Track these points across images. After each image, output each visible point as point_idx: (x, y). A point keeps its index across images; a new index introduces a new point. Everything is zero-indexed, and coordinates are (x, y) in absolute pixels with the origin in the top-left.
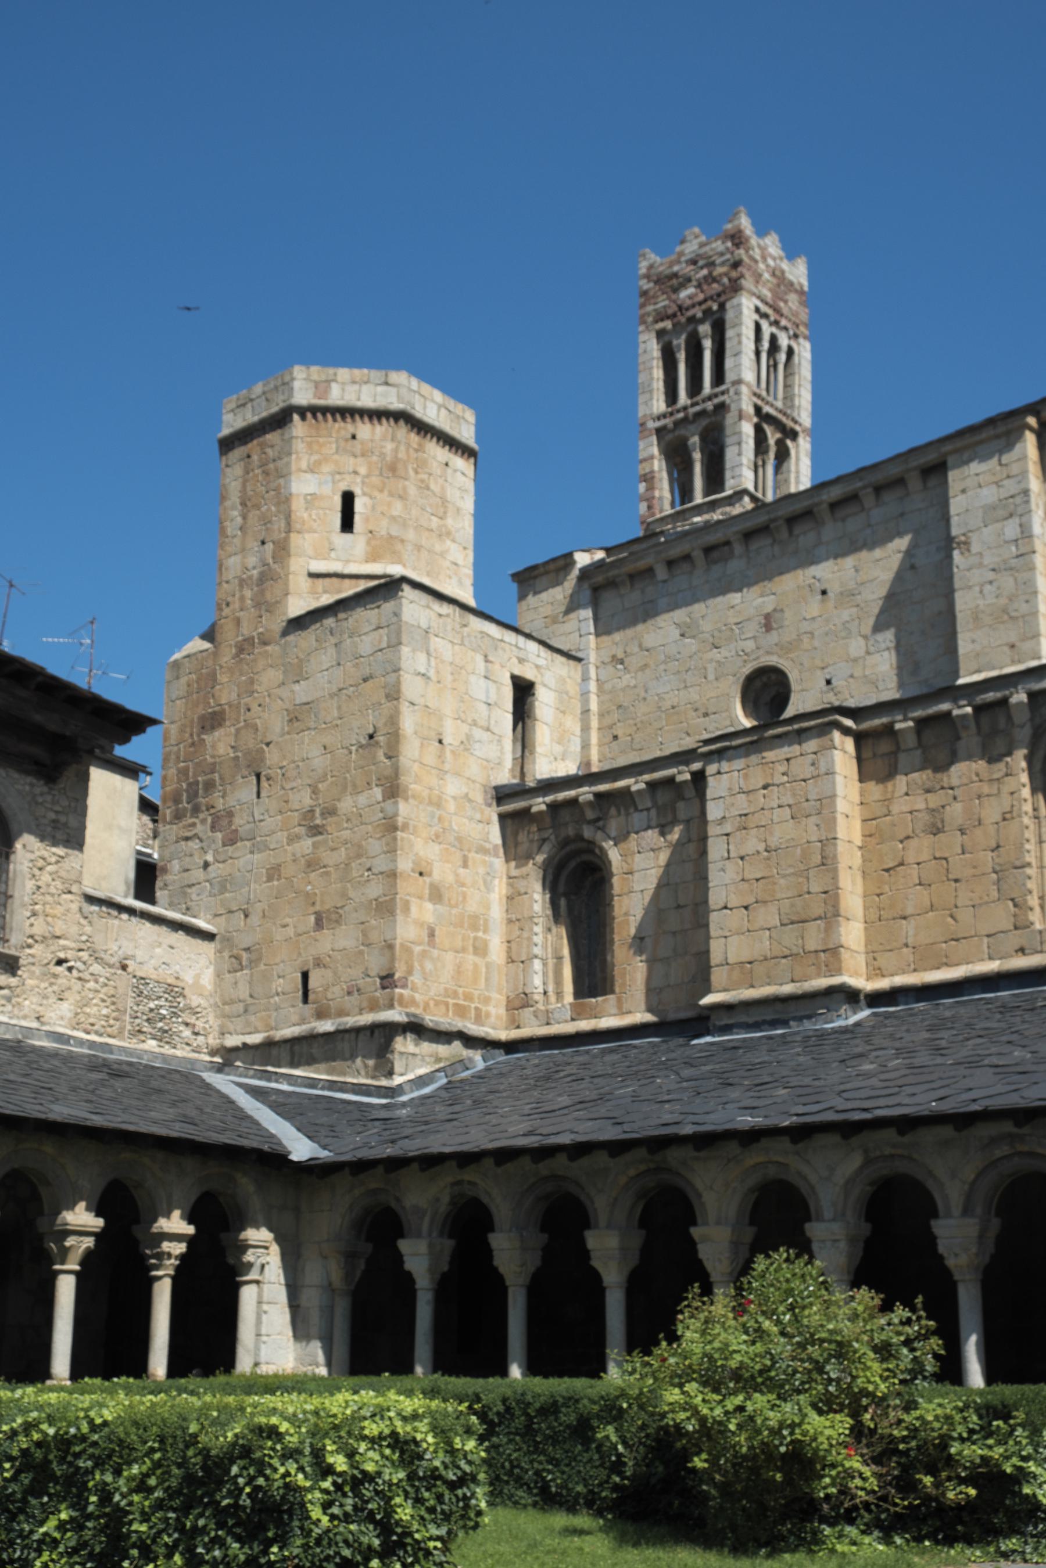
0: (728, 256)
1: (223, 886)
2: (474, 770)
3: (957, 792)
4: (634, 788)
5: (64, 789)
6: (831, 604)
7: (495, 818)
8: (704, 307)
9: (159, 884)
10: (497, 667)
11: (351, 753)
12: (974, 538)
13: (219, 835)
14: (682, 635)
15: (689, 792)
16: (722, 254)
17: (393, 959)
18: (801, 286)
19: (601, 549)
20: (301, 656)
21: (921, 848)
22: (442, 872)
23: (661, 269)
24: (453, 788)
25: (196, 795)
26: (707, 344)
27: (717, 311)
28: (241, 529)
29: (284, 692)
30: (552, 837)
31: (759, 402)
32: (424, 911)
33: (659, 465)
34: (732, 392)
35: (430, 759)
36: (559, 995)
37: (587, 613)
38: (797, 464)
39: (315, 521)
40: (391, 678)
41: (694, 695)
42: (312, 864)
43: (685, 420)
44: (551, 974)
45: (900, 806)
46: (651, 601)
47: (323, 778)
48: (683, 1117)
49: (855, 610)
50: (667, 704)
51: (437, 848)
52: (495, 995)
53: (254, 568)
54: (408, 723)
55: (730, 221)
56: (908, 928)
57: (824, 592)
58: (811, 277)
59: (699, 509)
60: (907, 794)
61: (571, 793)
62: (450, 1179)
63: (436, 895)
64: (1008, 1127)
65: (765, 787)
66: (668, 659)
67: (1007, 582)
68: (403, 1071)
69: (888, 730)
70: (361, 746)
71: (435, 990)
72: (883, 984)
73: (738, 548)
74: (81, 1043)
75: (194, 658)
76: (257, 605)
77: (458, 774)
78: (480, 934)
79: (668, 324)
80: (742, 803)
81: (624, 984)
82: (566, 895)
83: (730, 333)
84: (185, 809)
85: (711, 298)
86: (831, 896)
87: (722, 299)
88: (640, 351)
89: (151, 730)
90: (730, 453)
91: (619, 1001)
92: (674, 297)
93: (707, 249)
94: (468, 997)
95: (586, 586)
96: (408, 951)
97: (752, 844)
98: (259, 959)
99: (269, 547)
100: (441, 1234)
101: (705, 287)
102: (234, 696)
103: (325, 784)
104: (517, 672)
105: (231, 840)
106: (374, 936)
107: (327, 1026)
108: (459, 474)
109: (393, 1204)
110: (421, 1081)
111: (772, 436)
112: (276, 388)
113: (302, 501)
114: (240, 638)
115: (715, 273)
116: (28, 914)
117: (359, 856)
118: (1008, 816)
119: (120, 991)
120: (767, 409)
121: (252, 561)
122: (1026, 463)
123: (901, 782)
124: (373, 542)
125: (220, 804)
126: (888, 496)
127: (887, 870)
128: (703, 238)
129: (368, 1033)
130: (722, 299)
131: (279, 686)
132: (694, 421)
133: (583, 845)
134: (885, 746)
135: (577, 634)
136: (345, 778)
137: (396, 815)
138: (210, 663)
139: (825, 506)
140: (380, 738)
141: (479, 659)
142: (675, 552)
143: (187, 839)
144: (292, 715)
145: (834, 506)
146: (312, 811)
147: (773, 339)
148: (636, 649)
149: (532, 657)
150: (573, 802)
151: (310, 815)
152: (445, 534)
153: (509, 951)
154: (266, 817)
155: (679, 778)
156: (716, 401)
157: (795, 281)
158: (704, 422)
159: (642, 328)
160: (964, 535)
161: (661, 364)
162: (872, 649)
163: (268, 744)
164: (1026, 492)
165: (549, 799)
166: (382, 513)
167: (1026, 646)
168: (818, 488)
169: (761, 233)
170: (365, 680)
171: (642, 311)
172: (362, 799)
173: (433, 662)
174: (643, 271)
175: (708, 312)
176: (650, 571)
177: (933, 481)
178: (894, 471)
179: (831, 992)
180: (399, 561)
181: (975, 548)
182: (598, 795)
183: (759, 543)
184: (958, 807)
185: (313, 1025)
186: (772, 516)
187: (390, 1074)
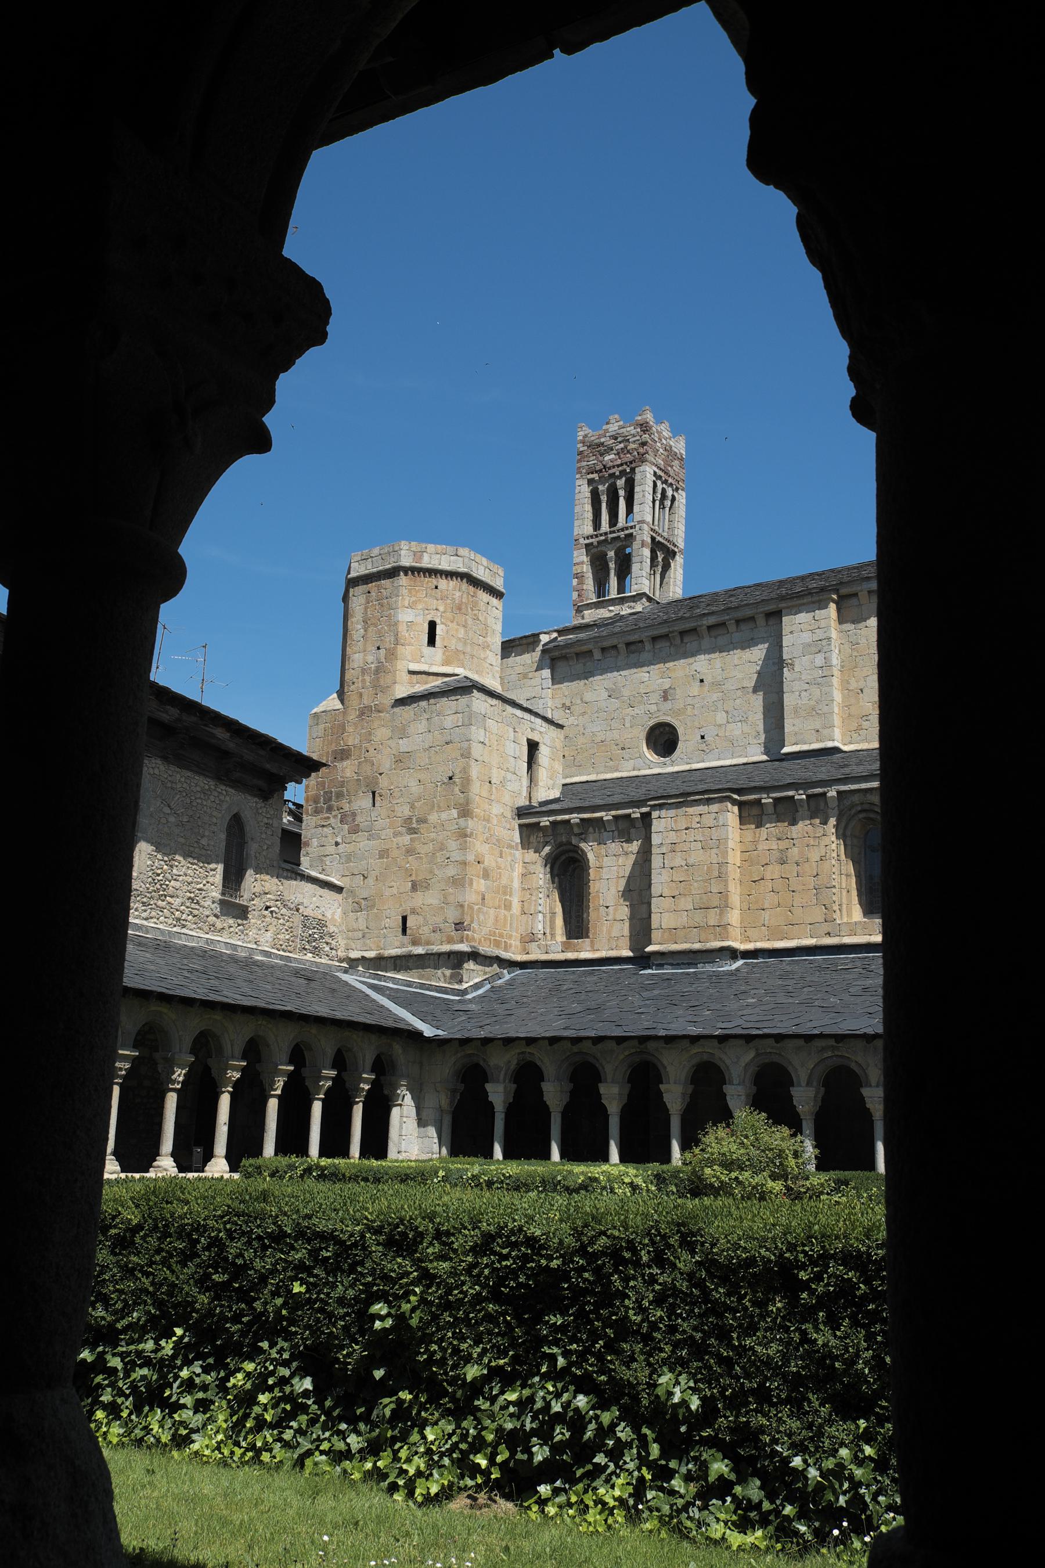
0: (638, 438)
1: (349, 858)
2: (507, 798)
3: (795, 842)
4: (605, 819)
6: (706, 689)
7: (517, 827)
9: (303, 852)
10: (520, 734)
12: (797, 662)
13: (346, 826)
15: (639, 824)
16: (634, 436)
17: (463, 914)
18: (681, 454)
19: (555, 631)
21: (774, 871)
22: (489, 861)
23: (592, 438)
24: (496, 810)
25: (330, 799)
26: (622, 493)
30: (552, 841)
31: (654, 535)
32: (480, 885)
33: (587, 569)
34: (637, 527)
35: (485, 794)
36: (553, 935)
37: (546, 673)
38: (675, 573)
40: (465, 745)
41: (615, 734)
42: (410, 851)
43: (606, 540)
44: (548, 923)
45: (763, 846)
48: (656, 1024)
50: (598, 739)
51: (487, 846)
52: (514, 934)
54: (474, 771)
56: (766, 916)
57: (702, 681)
58: (687, 448)
59: (613, 602)
60: (767, 839)
61: (567, 817)
62: (518, 1051)
63: (486, 875)
64: (832, 1042)
65: (686, 829)
67: (816, 692)
68: (467, 980)
69: (758, 802)
71: (485, 931)
72: (750, 946)
73: (648, 646)
74: (277, 956)
76: (375, 687)
77: (498, 802)
78: (508, 897)
79: (595, 476)
80: (672, 837)
81: (595, 933)
82: (557, 876)
83: (637, 489)
85: (626, 463)
86: (724, 895)
87: (633, 465)
88: (577, 491)
89: (323, 770)
90: (635, 568)
91: (592, 942)
92: (601, 458)
93: (623, 430)
94: (501, 935)
95: (547, 657)
96: (471, 908)
97: (678, 861)
98: (373, 906)
99: (382, 651)
100: (510, 1081)
101: (622, 456)
102: (357, 741)
105: (355, 830)
106: (451, 899)
107: (420, 950)
109: (481, 1063)
110: (477, 986)
112: (389, 553)
115: (629, 448)
116: (253, 880)
117: (441, 849)
118: (823, 858)
119: (295, 924)
120: (658, 538)
121: (370, 658)
122: (830, 621)
123: (763, 832)
125: (346, 807)
126: (744, 627)
127: (754, 882)
128: (621, 423)
129: (446, 957)
130: (633, 465)
132: (610, 543)
133: (572, 848)
134: (755, 811)
135: (540, 687)
137: (467, 827)
138: (341, 718)
139: (705, 627)
141: (511, 730)
142: (606, 644)
143: (323, 826)
145: (710, 628)
146: (410, 819)
147: (664, 491)
148: (579, 702)
150: (568, 821)
151: (409, 821)
152: (486, 647)
153: (523, 907)
154: (379, 818)
155: (633, 816)
156: (627, 532)
159: (578, 476)
162: (730, 720)
163: (381, 774)
164: (829, 639)
165: (551, 819)
167: (825, 732)
168: (690, 602)
169: (659, 422)
171: (579, 465)
172: (444, 816)
174: (581, 438)
175: (623, 473)
176: (590, 652)
178: (748, 612)
179: (722, 949)
181: (797, 669)
182: (582, 820)
183: (662, 644)
184: (795, 850)
185: (410, 948)
187: (461, 981)
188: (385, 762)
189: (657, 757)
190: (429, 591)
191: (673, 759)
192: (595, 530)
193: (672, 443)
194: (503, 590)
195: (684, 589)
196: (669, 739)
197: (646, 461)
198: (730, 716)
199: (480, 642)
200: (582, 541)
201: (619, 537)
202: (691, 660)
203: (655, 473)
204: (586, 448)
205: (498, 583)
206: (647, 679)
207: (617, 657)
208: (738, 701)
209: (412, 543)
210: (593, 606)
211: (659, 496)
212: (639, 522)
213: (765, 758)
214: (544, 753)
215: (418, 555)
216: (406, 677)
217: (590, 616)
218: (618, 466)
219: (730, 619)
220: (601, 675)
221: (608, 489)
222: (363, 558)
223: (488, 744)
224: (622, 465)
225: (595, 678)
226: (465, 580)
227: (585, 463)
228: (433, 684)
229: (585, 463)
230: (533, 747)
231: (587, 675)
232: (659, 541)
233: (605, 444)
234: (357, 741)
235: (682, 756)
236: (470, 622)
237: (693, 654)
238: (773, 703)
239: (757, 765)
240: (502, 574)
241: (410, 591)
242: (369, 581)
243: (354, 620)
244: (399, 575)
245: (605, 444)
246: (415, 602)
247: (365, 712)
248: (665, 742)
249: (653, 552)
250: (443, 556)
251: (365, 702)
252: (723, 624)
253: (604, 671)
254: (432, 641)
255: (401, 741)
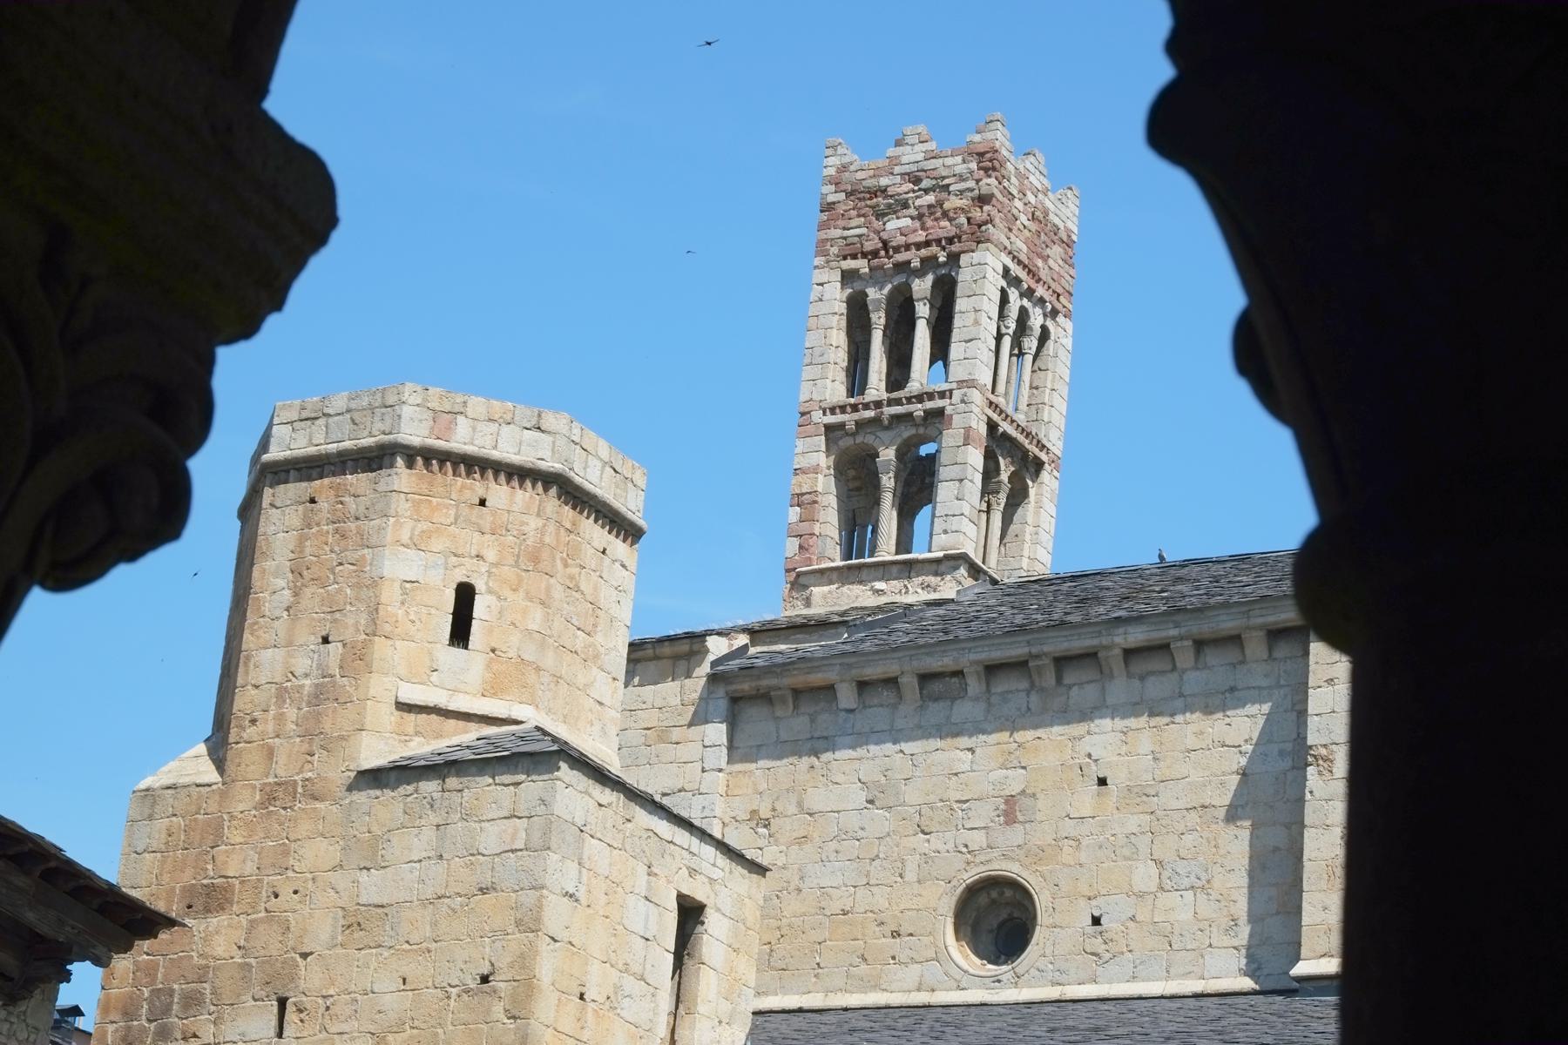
0: (971, 184)
5: (25, 1013)
8: (924, 252)
10: (662, 882)
11: (449, 998)
14: (871, 802)
16: (962, 179)
18: (1069, 232)
19: (745, 630)
20: (374, 829)
23: (860, 175)
25: (167, 1010)
26: (923, 310)
27: (944, 264)
28: (288, 609)
29: (340, 879)
31: (995, 417)
33: (825, 486)
34: (957, 395)
37: (717, 732)
38: (1037, 514)
39: (414, 622)
40: (529, 898)
41: (880, 899)
43: (876, 421)
46: (826, 738)
47: (398, 1028)
49: (1148, 817)
50: (836, 907)
53: (306, 675)
54: (547, 966)
55: (978, 132)
57: (1102, 782)
66: (843, 835)
70: (467, 991)
73: (974, 685)
75: (184, 792)
79: (861, 265)
83: (961, 304)
84: (143, 1030)
85: (938, 241)
87: (955, 248)
89: (164, 936)
90: (945, 492)
92: (877, 224)
95: (721, 691)
99: (335, 649)
101: (929, 223)
102: (250, 868)
103: (399, 1037)
104: (685, 891)
108: (617, 564)
111: (1006, 470)
113: (397, 585)
114: (271, 780)
115: (947, 206)
120: (1004, 426)
121: (302, 663)
124: (495, 667)
126: (1212, 657)
128: (932, 146)
130: (955, 248)
131: (334, 869)
132: (887, 428)
135: (698, 766)
136: (436, 1034)
138: (213, 807)
139: (1117, 651)
140: (497, 983)
142: (873, 672)
144: (352, 920)
145: (1129, 653)
147: (1023, 315)
148: (792, 809)
149: (705, 867)
152: (590, 658)
156: (929, 405)
157: (1061, 226)
158: (907, 432)
159: (819, 261)
160: (1325, 746)
161: (844, 323)
162: (1168, 884)
163: (305, 956)
166: (514, 624)
170: (483, 891)
171: (823, 235)
173: (585, 879)
174: (832, 171)
175: (929, 263)
176: (830, 689)
177: (1284, 649)
178: (1227, 623)
180: (533, 703)
186: (1034, 650)
188: (321, 929)
189: (977, 961)
190: (465, 510)
191: (1019, 970)
192: (851, 393)
193: (1048, 204)
194: (641, 523)
195: (1055, 554)
196: (1011, 919)
197: (988, 240)
198: (1166, 874)
199: (579, 646)
200: (817, 416)
201: (910, 415)
202: (1078, 729)
203: (1006, 271)
204: (842, 196)
205: (631, 505)
206: (966, 767)
207: (894, 707)
208: (1188, 838)
209: (432, 390)
210: (835, 575)
211: (1013, 326)
212: (962, 383)
213: (1247, 984)
214: (714, 932)
215: (444, 418)
216: (390, 716)
217: (826, 600)
218: (919, 246)
219: (1182, 638)
220: (853, 747)
221: (890, 299)
222: (305, 414)
223: (584, 902)
224: (927, 244)
225: (838, 754)
226: (553, 491)
227: (838, 233)
228: (455, 741)
229: (838, 233)
230: (690, 913)
231: (817, 744)
232: (1005, 435)
233: (891, 191)
234: (250, 868)
235: (1041, 963)
236: (558, 593)
237: (1085, 715)
238: (1276, 849)
239: (1229, 1000)
240: (641, 481)
241: (417, 504)
242: (314, 473)
243: (269, 565)
244: (392, 466)
245: (891, 191)
246: (425, 535)
247: (275, 796)
248: (1001, 925)
249: (990, 457)
250: (505, 428)
251: (281, 772)
252: (1163, 648)
253: (861, 738)
254: (460, 633)
255: (364, 877)
